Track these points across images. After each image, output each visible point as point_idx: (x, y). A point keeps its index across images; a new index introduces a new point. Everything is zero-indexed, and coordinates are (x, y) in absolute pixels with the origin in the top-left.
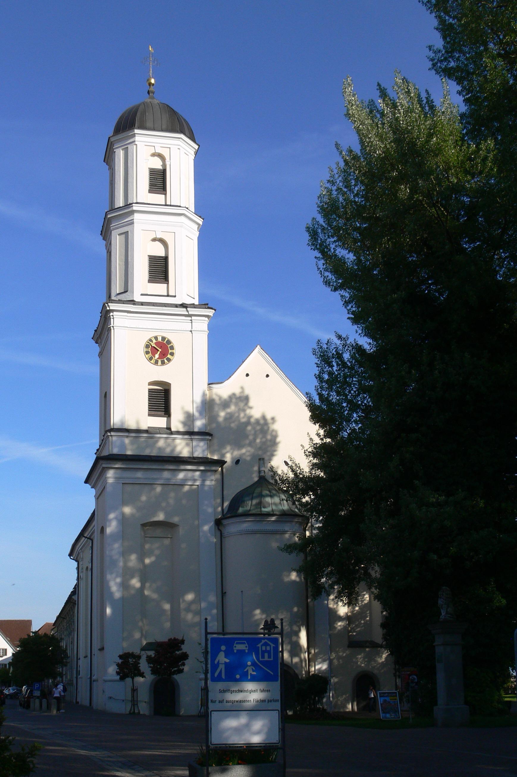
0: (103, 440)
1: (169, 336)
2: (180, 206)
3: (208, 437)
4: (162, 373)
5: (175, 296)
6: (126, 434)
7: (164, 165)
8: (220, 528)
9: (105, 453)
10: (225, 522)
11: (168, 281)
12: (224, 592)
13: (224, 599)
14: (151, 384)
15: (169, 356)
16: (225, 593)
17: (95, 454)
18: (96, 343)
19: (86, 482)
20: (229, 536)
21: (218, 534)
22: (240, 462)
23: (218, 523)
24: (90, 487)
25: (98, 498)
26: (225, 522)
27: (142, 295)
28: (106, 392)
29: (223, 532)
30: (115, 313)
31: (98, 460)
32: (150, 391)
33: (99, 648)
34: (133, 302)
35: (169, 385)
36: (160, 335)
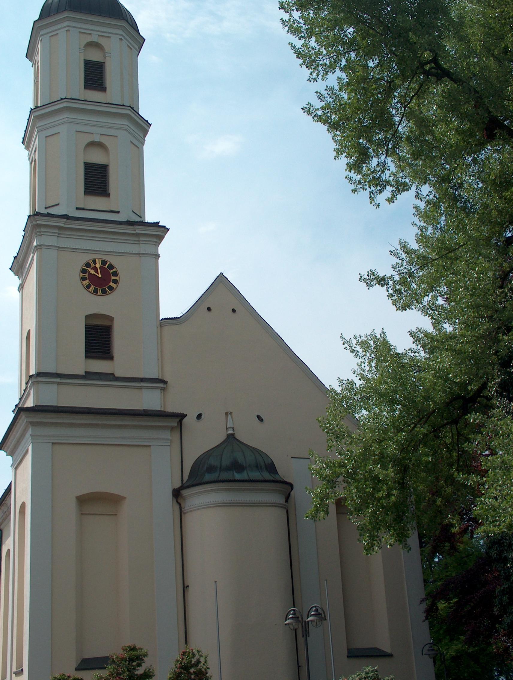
1: (111, 260)
2: (123, 105)
3: (161, 385)
4: (100, 305)
6: (58, 380)
9: (30, 403)
10: (185, 493)
11: (109, 194)
12: (186, 585)
13: (186, 593)
14: (87, 317)
15: (112, 284)
16: (188, 586)
17: (13, 411)
20: (191, 511)
21: (177, 508)
22: (203, 417)
23: (177, 494)
24: (5, 453)
26: (185, 493)
27: (77, 209)
35: (111, 319)
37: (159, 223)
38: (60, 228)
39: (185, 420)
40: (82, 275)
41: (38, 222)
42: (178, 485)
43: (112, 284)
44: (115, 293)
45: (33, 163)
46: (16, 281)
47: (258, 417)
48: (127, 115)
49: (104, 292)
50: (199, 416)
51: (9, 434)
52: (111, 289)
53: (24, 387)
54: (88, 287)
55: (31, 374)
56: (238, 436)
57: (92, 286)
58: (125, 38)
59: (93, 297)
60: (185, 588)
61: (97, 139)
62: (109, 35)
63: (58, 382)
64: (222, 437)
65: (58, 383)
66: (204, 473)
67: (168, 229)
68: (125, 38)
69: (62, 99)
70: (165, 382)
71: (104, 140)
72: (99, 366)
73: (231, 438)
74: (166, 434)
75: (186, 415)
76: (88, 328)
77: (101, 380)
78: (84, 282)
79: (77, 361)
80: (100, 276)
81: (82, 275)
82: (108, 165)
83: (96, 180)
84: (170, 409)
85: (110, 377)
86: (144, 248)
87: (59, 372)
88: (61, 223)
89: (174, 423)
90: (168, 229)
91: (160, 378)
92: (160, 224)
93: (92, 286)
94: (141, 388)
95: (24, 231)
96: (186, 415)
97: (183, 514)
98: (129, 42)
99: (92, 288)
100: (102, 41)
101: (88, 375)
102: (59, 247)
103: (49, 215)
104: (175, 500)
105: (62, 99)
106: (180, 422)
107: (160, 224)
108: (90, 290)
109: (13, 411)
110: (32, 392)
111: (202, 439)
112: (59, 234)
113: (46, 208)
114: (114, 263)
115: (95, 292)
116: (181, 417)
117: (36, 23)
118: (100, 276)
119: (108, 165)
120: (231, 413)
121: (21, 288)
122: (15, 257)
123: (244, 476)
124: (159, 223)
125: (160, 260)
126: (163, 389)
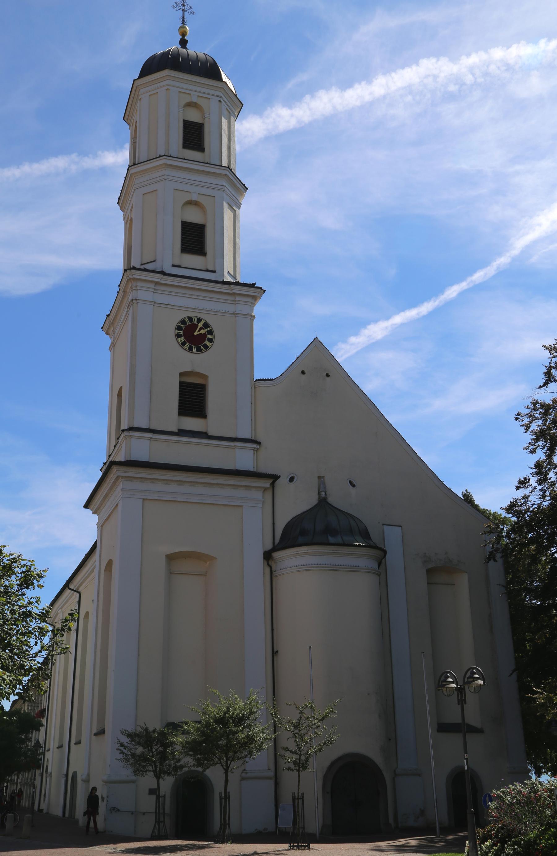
0: (109, 456)
1: (206, 318)
3: (254, 446)
5: (214, 272)
6: (150, 435)
7: (204, 118)
8: (270, 563)
9: (120, 458)
10: (276, 555)
12: (275, 650)
13: (275, 659)
14: (182, 374)
15: (207, 343)
16: (277, 652)
17: (101, 470)
18: (107, 333)
19: (86, 506)
21: (268, 570)
22: (295, 480)
23: (268, 556)
25: (102, 526)
28: (121, 387)
29: (274, 569)
30: (139, 284)
31: (109, 467)
32: (181, 384)
33: (95, 731)
34: (163, 273)
35: (205, 377)
36: (195, 315)
37: (255, 284)
38: (157, 283)
39: (278, 482)
40: (178, 332)
41: (135, 276)
42: (269, 546)
43: (207, 343)
44: (210, 351)
45: (129, 222)
46: (108, 340)
47: (350, 482)
48: (227, 175)
49: (199, 350)
50: (292, 479)
51: (136, 428)
52: (206, 347)
53: (113, 444)
54: (183, 344)
55: (122, 428)
56: (330, 500)
57: (187, 344)
58: (224, 100)
59: (189, 354)
60: (274, 653)
61: (195, 198)
62: (209, 96)
63: (151, 438)
64: (313, 501)
65: (151, 439)
66: (295, 534)
67: (264, 291)
68: (224, 100)
69: (160, 156)
70: (259, 443)
71: (201, 199)
72: (192, 423)
73: (323, 502)
74: (258, 495)
75: (279, 477)
76: (182, 385)
77: (194, 437)
78: (179, 339)
79: (170, 418)
80: (196, 333)
81: (178, 332)
82: (205, 225)
83: (194, 238)
84: (263, 469)
85: (204, 435)
86: (241, 308)
87: (152, 427)
88: (158, 278)
89: (267, 483)
90: (264, 291)
91: (253, 438)
92: (256, 286)
93: (187, 344)
94: (234, 447)
95: (119, 286)
96: (279, 477)
97: (273, 577)
98: (227, 105)
99: (187, 345)
100: (201, 102)
101: (181, 433)
102: (155, 303)
103: (145, 270)
104: (266, 563)
105: (160, 156)
106: (273, 485)
107: (256, 286)
108: (185, 347)
109: (101, 470)
110: (123, 446)
111: (294, 501)
112: (155, 289)
113: (142, 265)
114: (210, 322)
115: (190, 349)
116: (275, 478)
117: (135, 81)
118: (196, 333)
119: (205, 225)
120: (323, 477)
121: (113, 346)
122: (108, 316)
123: (339, 539)
124: (255, 284)
125: (255, 322)
126: (256, 450)
